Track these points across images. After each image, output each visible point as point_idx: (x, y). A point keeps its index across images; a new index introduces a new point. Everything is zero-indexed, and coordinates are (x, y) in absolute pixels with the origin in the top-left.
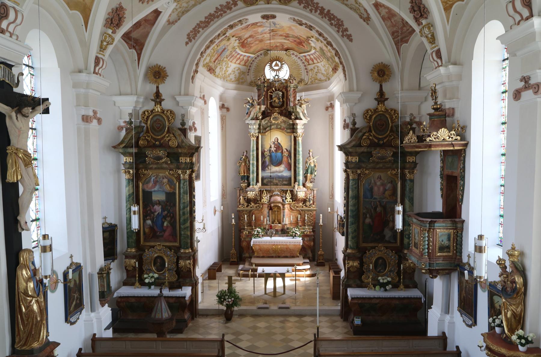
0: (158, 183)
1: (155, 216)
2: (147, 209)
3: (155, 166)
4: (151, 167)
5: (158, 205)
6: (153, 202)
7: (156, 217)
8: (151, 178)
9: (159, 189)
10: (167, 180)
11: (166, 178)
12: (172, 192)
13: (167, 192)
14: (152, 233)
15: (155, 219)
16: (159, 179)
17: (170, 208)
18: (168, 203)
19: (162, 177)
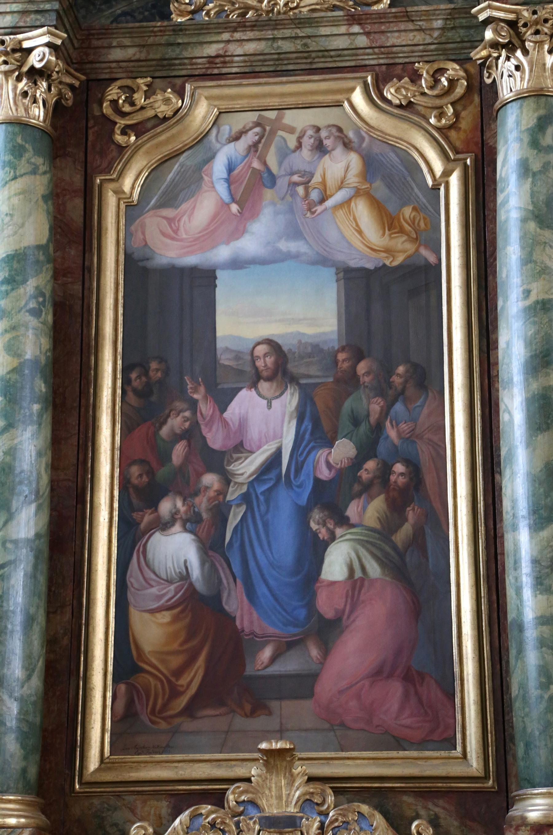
0: (268, 194)
1: (233, 494)
2: (165, 431)
3: (251, 47)
4: (211, 59)
5: (264, 386)
6: (224, 359)
7: (246, 498)
8: (211, 158)
9: (285, 246)
10: (354, 159)
11: (347, 145)
12: (400, 259)
13: (354, 263)
14: (201, 661)
15: (233, 521)
16: (284, 154)
17: (385, 413)
18: (362, 367)
19: (308, 142)
